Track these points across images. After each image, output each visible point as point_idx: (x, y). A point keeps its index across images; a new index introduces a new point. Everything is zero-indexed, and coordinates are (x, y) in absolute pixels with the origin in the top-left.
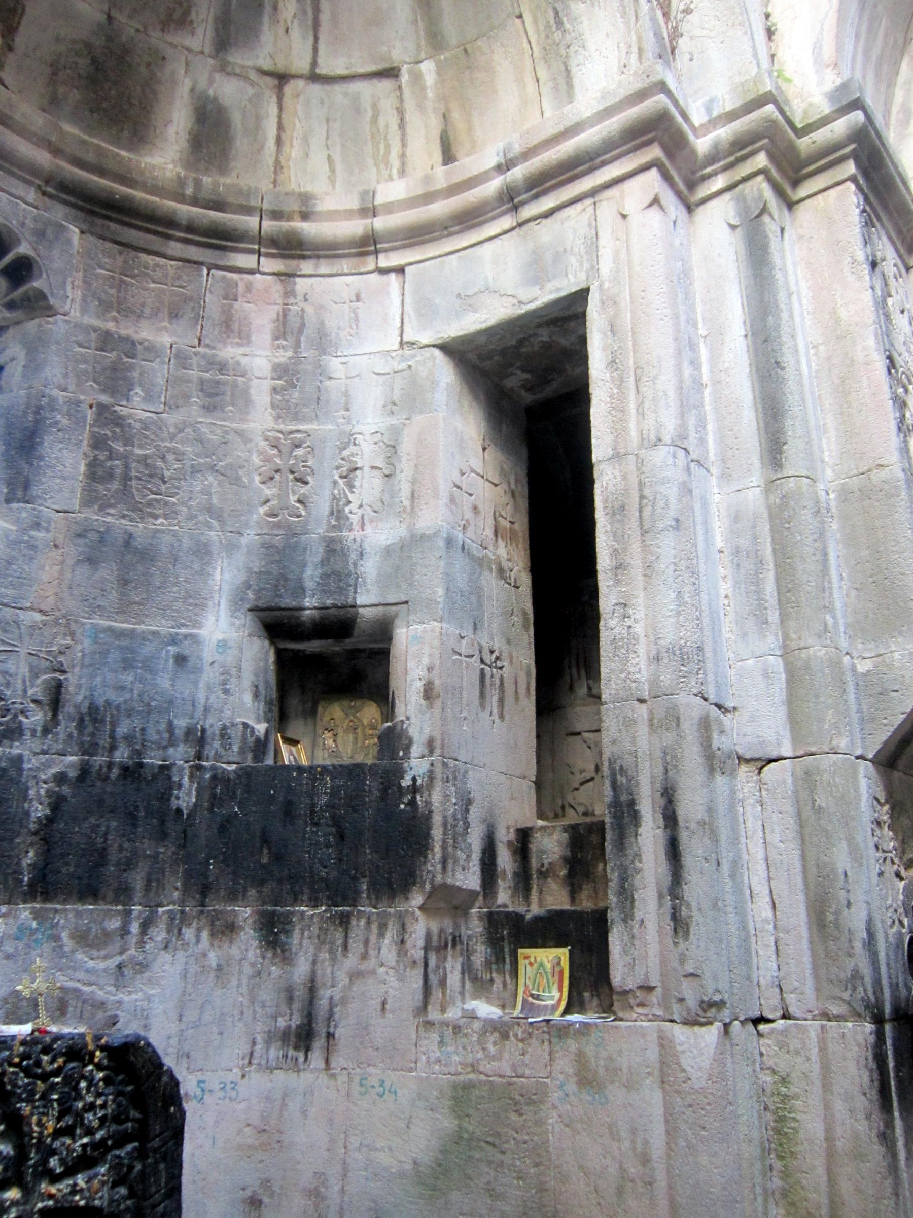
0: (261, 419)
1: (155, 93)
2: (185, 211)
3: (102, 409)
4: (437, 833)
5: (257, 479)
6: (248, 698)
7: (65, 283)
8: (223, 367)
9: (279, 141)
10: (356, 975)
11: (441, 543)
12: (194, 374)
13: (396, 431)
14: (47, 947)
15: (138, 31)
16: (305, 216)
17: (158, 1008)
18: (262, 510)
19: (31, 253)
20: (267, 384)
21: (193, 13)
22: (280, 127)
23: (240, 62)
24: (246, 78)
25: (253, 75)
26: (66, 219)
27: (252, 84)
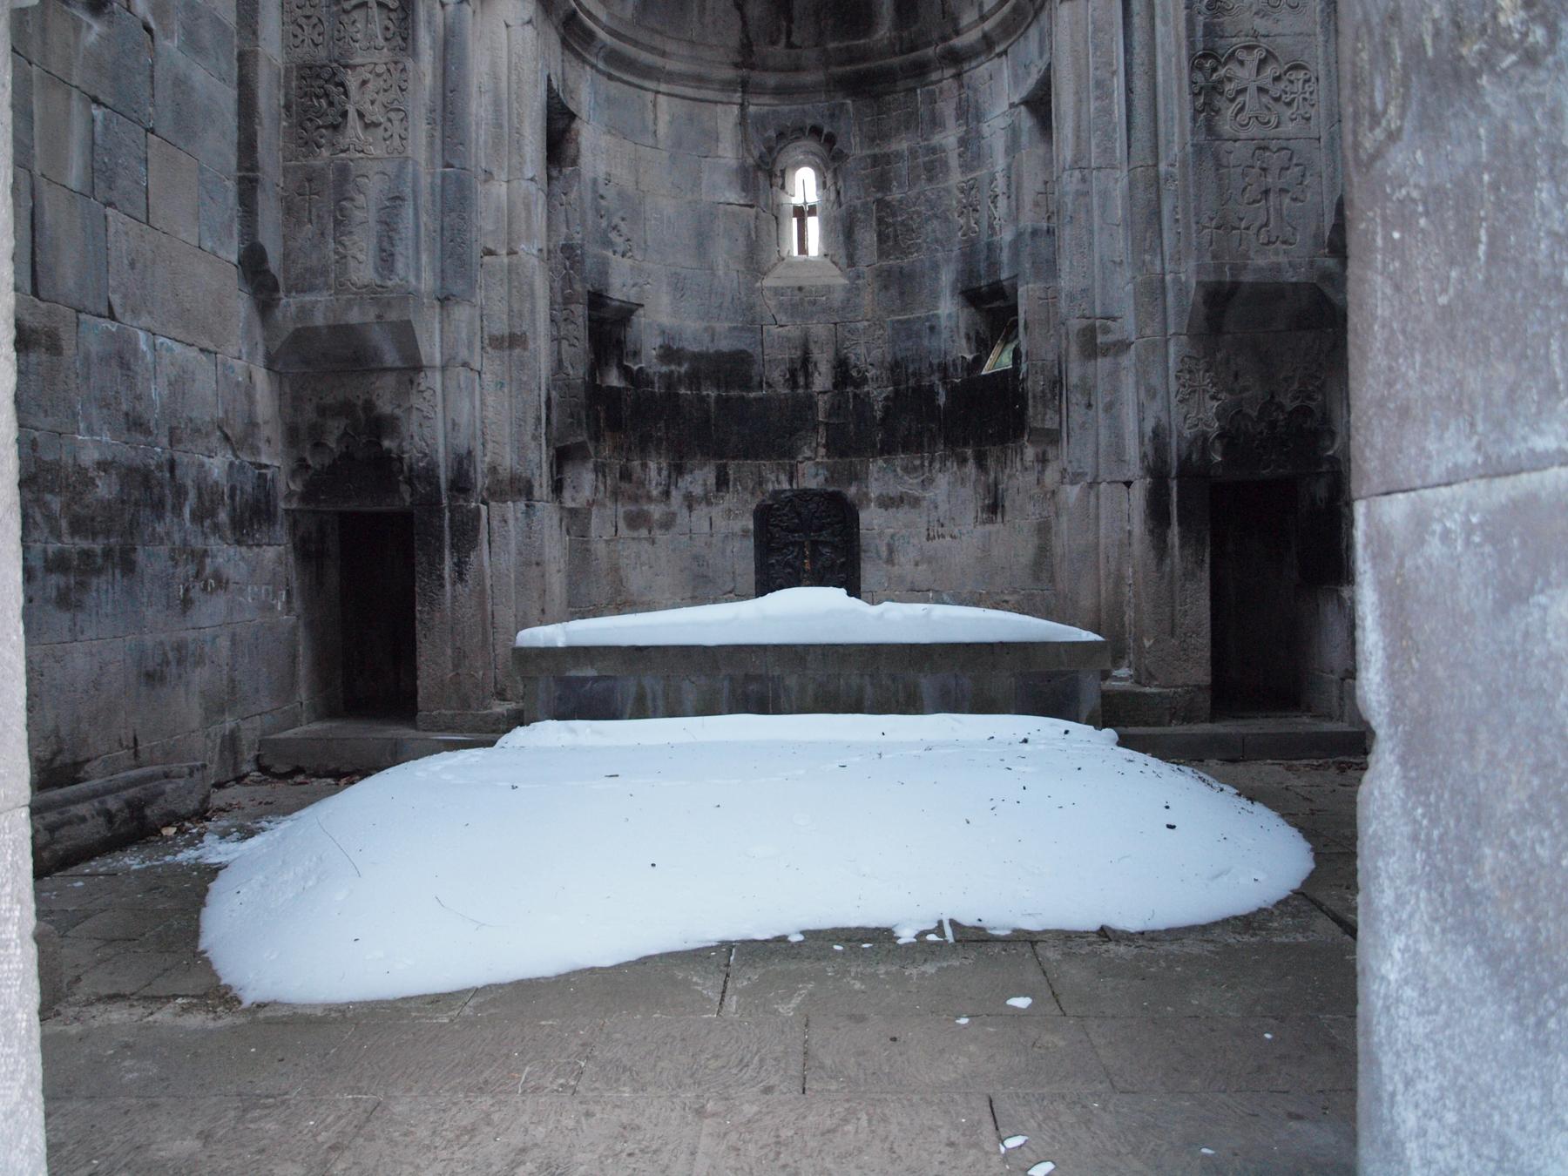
0: (956, 178)
2: (896, 61)
3: (879, 202)
4: (1030, 402)
6: (964, 342)
8: (933, 150)
10: (1010, 477)
11: (1027, 236)
12: (919, 160)
13: (1009, 167)
14: (891, 475)
16: (958, 33)
17: (940, 499)
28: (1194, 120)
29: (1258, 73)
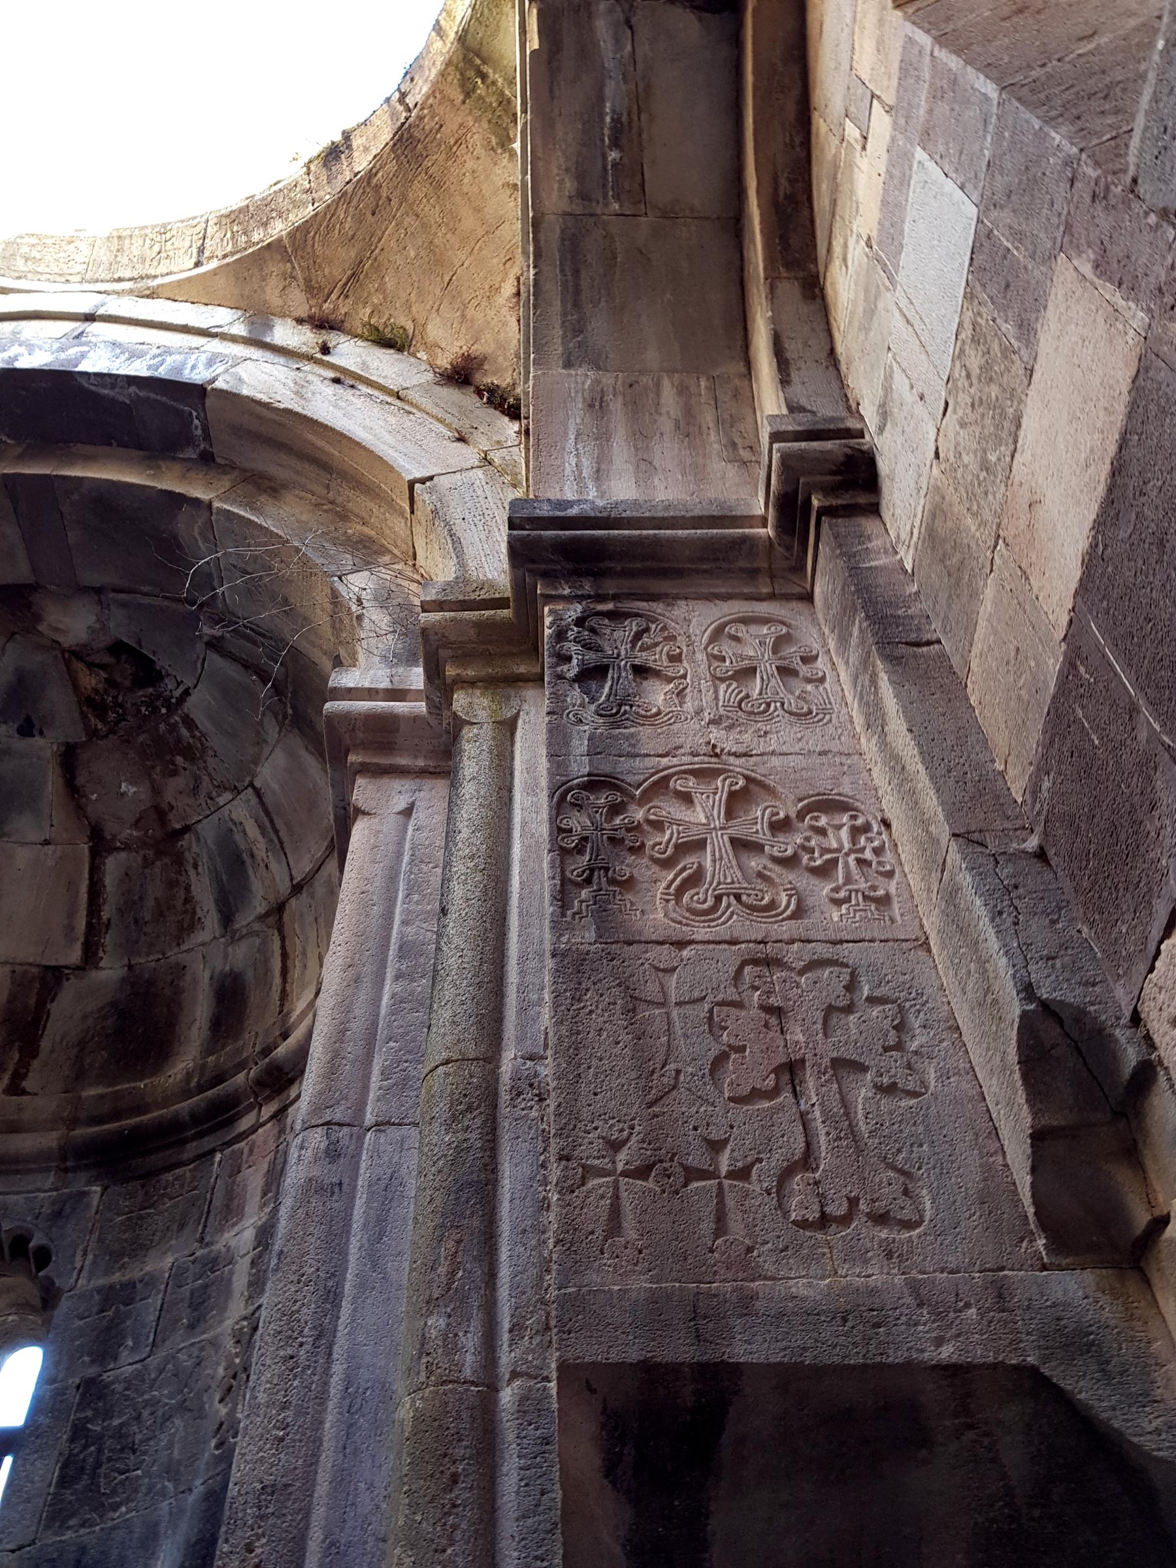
1: (179, 1004)
5: (217, 1397)
7: (74, 1255)
8: (213, 1263)
9: (284, 972)
15: (159, 960)
18: (213, 1443)
19: (44, 1241)
20: (247, 1260)
21: (198, 910)
22: (285, 956)
23: (244, 923)
24: (252, 933)
25: (257, 927)
26: (89, 1183)
27: (257, 934)
28: (562, 897)
29: (730, 814)
